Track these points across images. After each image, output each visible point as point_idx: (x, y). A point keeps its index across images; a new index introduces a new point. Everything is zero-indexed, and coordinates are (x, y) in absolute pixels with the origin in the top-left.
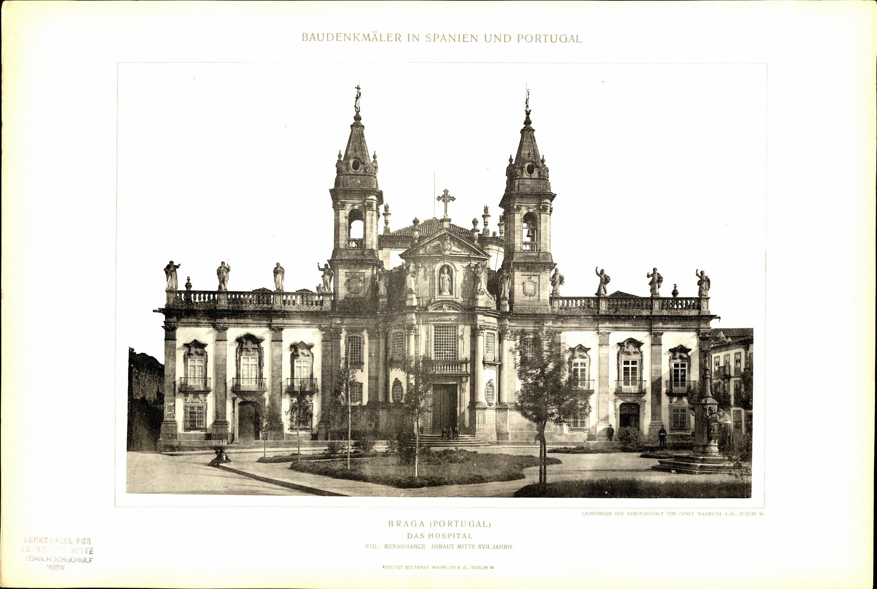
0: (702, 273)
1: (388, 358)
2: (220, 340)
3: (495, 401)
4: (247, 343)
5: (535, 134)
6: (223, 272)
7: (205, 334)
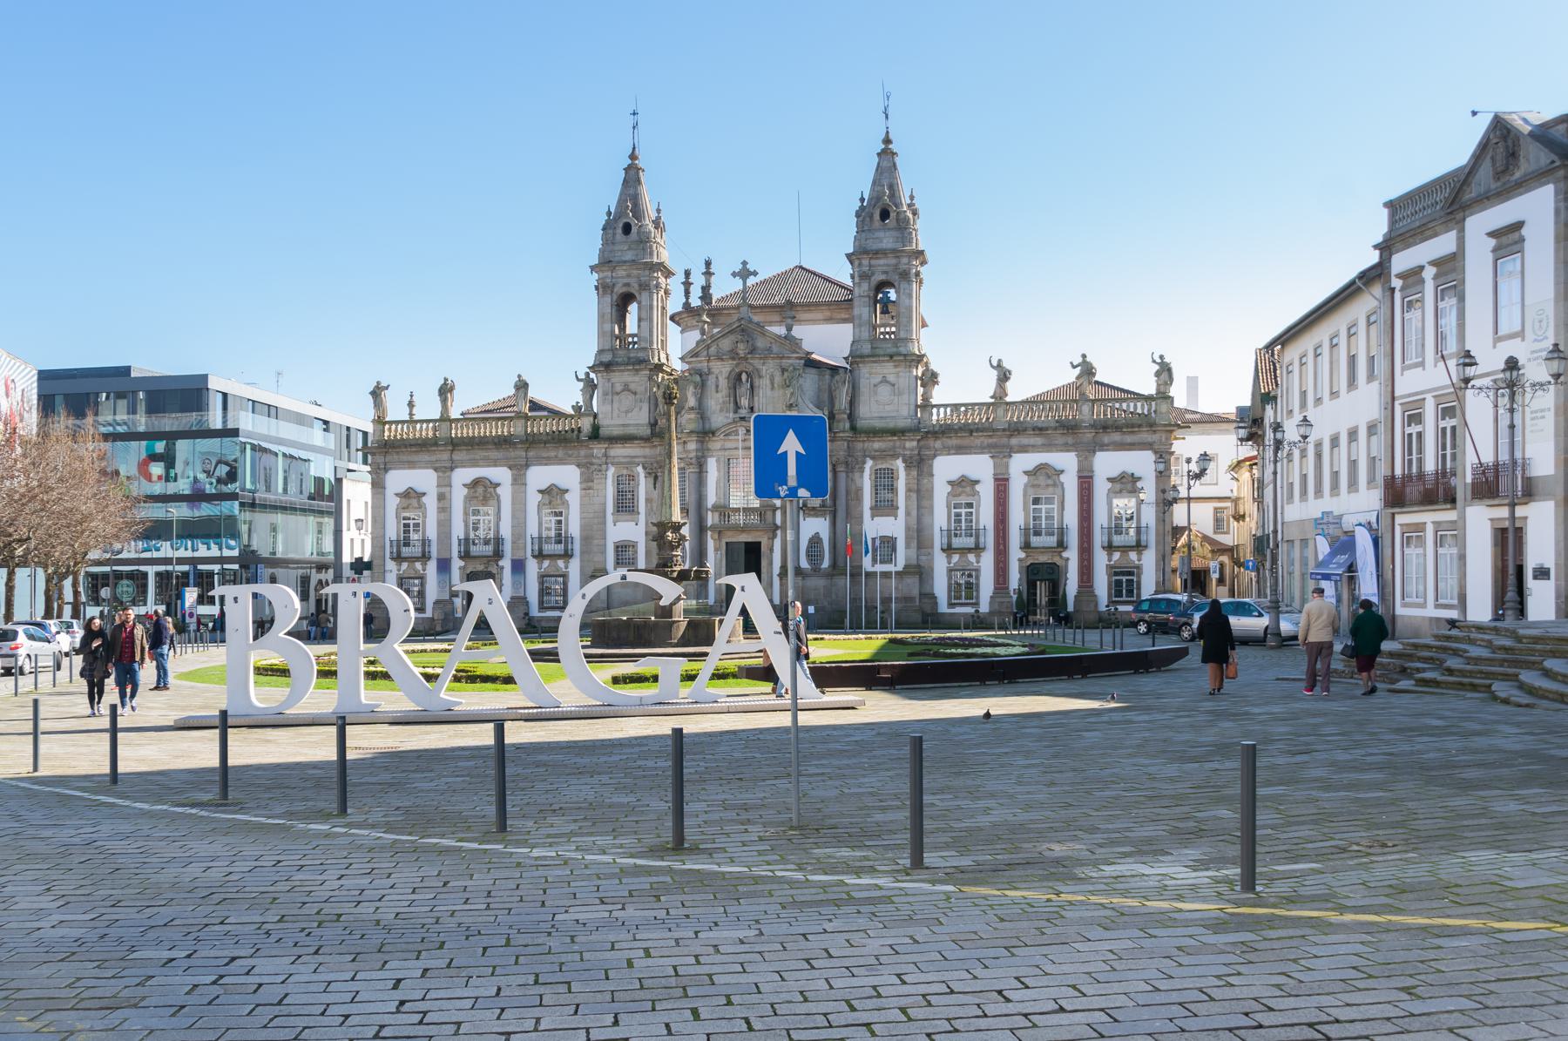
0: (1161, 357)
2: (445, 483)
3: (826, 564)
4: (482, 491)
5: (898, 160)
6: (445, 391)
7: (423, 479)
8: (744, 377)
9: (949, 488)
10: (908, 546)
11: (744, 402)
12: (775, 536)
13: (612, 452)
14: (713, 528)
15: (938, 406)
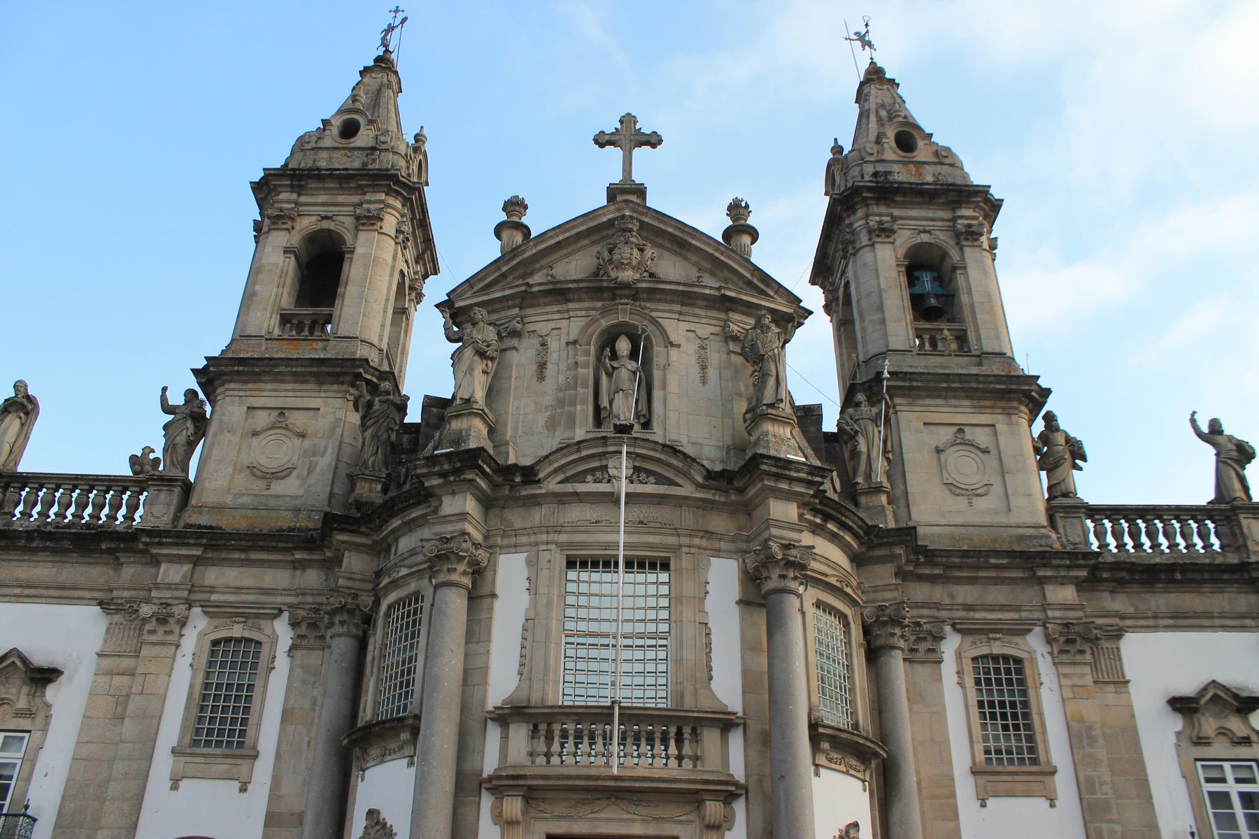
1: (360, 724)
8: (623, 346)
9: (1177, 723)
11: (625, 409)
12: (728, 822)
13: (211, 575)
14: (501, 785)
15: (1096, 512)
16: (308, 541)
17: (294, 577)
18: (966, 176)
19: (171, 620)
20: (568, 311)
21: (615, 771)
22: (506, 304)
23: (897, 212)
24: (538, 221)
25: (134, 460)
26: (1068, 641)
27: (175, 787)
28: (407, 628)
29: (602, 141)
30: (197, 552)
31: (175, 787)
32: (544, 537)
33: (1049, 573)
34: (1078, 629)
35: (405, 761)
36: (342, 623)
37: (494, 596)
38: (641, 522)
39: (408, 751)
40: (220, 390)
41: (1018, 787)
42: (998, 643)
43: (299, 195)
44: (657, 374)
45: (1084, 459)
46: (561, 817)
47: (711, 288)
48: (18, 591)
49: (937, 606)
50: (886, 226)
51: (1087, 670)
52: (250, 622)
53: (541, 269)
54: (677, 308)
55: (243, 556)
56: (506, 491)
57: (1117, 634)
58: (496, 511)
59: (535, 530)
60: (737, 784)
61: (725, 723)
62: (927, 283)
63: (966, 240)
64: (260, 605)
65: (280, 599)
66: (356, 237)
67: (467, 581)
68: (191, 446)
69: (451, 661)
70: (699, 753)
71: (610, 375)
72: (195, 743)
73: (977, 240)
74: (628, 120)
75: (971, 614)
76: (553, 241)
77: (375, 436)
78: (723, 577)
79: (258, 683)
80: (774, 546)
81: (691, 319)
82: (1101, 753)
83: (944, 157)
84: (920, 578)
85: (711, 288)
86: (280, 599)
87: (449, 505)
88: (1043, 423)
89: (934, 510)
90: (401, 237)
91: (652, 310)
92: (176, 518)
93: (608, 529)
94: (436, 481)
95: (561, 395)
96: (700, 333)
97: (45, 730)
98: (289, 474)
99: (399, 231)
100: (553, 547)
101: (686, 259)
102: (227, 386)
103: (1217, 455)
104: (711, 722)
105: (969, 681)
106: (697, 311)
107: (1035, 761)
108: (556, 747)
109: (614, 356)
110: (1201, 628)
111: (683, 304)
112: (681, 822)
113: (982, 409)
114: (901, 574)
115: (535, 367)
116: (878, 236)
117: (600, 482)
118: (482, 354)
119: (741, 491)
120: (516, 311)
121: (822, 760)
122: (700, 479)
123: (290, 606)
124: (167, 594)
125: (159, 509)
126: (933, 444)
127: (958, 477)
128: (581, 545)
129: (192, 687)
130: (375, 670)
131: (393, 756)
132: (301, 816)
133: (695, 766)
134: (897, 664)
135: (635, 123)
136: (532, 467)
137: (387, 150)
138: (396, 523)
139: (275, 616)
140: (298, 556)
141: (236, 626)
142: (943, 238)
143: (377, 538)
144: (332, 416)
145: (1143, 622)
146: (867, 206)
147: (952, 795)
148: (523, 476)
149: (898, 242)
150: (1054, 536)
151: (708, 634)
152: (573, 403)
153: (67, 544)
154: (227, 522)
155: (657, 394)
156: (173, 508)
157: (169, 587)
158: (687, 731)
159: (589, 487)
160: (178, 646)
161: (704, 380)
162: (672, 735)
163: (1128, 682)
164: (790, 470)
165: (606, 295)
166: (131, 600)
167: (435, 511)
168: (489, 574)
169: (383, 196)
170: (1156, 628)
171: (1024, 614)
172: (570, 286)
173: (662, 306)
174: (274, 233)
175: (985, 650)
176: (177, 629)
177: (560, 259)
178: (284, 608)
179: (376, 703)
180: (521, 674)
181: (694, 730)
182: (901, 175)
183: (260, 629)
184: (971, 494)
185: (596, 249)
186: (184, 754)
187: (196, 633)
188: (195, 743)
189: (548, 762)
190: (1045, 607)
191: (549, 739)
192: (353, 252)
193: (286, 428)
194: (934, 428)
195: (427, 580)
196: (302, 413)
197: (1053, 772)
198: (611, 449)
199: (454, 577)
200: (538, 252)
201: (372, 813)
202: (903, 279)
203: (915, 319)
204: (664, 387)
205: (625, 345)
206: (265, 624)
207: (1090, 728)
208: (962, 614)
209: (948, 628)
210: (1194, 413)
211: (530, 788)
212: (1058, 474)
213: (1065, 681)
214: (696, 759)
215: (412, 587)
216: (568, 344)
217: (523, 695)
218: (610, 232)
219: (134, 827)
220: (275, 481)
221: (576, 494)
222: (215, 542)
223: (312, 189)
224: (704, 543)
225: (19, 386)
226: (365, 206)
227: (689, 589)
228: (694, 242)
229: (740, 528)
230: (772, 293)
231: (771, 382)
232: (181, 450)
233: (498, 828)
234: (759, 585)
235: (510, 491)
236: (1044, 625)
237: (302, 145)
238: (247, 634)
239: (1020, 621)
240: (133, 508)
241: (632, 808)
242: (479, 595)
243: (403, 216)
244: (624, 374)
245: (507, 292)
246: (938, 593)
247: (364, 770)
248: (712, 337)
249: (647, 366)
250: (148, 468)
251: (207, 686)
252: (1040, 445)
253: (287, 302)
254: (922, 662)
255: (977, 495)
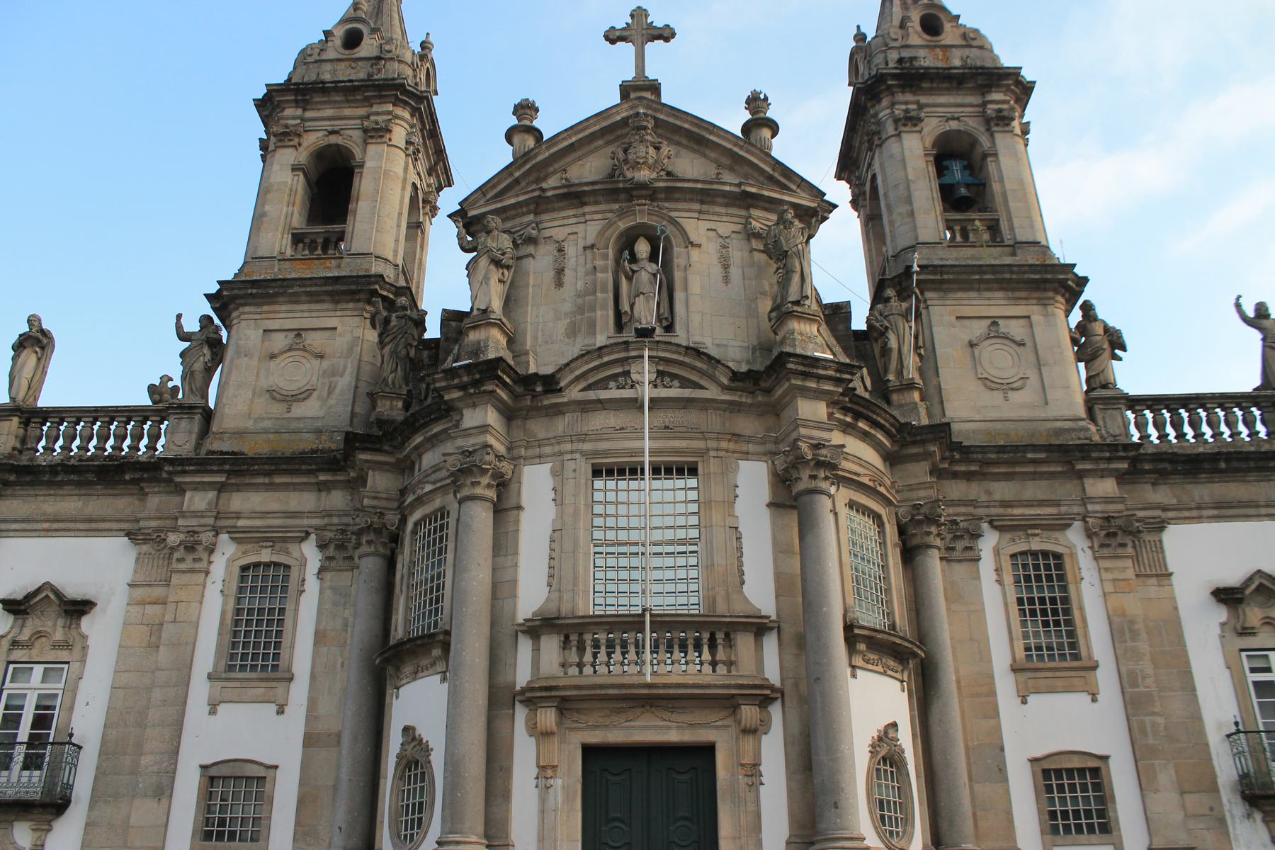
1: (392, 642)
8: (643, 248)
9: (1222, 614)
10: (1145, 783)
11: (646, 312)
13: (236, 501)
14: (534, 697)
15: (1136, 403)
16: (332, 462)
17: (319, 499)
18: (995, 58)
19: (200, 548)
20: (584, 214)
21: (649, 679)
22: (520, 211)
23: (923, 100)
24: (549, 125)
25: (152, 389)
26: (1108, 535)
27: (213, 712)
28: (434, 544)
29: (613, 37)
30: (221, 478)
31: (213, 712)
32: (568, 447)
33: (1088, 466)
34: (1119, 522)
35: (438, 677)
36: (369, 542)
37: (519, 508)
38: (666, 427)
39: (440, 666)
40: (235, 314)
41: (1059, 683)
42: (1037, 539)
43: (304, 110)
44: (678, 275)
45: (1124, 349)
46: (596, 727)
47: (731, 184)
48: (46, 525)
49: (973, 503)
50: (913, 114)
51: (1129, 563)
52: (278, 545)
53: (555, 172)
54: (697, 206)
55: (267, 480)
56: (528, 401)
57: (1160, 526)
58: (519, 422)
59: (559, 440)
60: (772, 688)
61: (759, 628)
62: (956, 172)
63: (997, 125)
64: (286, 529)
65: (306, 522)
66: (365, 151)
67: (491, 494)
68: (209, 372)
69: (478, 575)
70: (733, 658)
71: (630, 279)
72: (231, 668)
73: (1008, 125)
74: (639, 14)
75: (1009, 511)
76: (566, 143)
77: (394, 353)
78: (753, 479)
79: (289, 607)
80: (804, 447)
81: (711, 217)
82: (1143, 646)
83: (972, 39)
84: (955, 475)
85: (731, 184)
86: (306, 522)
87: (471, 418)
88: (1080, 313)
89: (969, 405)
90: (411, 148)
91: (671, 210)
92: (198, 445)
93: (634, 435)
94: (456, 394)
95: (580, 301)
96: (721, 231)
97: (83, 660)
98: (309, 396)
99: (408, 143)
100: (577, 456)
101: (704, 156)
102: (241, 310)
103: (1264, 340)
104: (744, 627)
105: (1008, 579)
106: (718, 209)
107: (1076, 657)
108: (588, 657)
109: (634, 259)
110: (1247, 517)
111: (702, 202)
112: (717, 727)
113: (1016, 301)
114: (936, 472)
115: (552, 274)
116: (905, 125)
117: (623, 387)
118: (497, 263)
119: (768, 391)
120: (531, 217)
121: (858, 661)
122: (725, 381)
123: (317, 528)
124: (194, 522)
125: (180, 438)
126: (966, 338)
127: (993, 372)
128: (606, 453)
129: (223, 613)
130: (404, 588)
131: (426, 673)
132: (339, 735)
133: (729, 671)
134: (933, 564)
135: (647, 16)
136: (553, 376)
137: (392, 59)
138: (418, 439)
139: (303, 539)
140: (322, 477)
141: (264, 551)
142: (973, 125)
143: (401, 456)
144: (350, 335)
145: (1186, 514)
146: (892, 94)
147: (993, 693)
148: (544, 385)
149: (926, 130)
150: (1093, 428)
151: (739, 539)
152: (593, 309)
153: (91, 477)
154: (249, 447)
155: (679, 296)
156: (194, 436)
157: (195, 514)
158: (720, 636)
159: (613, 393)
160: (207, 573)
161: (726, 279)
162: (705, 641)
163: (1171, 574)
164: (818, 368)
165: (622, 196)
166: (158, 530)
167: (457, 426)
168: (514, 486)
169: (390, 107)
170: (1199, 519)
171: (1063, 509)
172: (586, 188)
173: (680, 206)
174: (281, 152)
175: (1023, 547)
176: (205, 556)
177: (574, 161)
178: (310, 530)
179: (407, 622)
180: (550, 585)
181: (727, 635)
182: (927, 60)
183: (287, 553)
184: (1007, 388)
185: (610, 149)
186: (219, 679)
187: (225, 558)
188: (231, 668)
189: (581, 672)
190: (1084, 501)
191: (581, 649)
192: (362, 166)
193: (304, 349)
194: (967, 322)
195: (452, 495)
196: (319, 333)
197: (1095, 667)
198: (633, 353)
199: (478, 491)
200: (552, 155)
201: (407, 730)
202: (932, 169)
203: (945, 210)
204: (686, 289)
205: (645, 247)
206: (292, 547)
207: (1132, 622)
208: (1000, 511)
209: (985, 526)
210: (1239, 297)
211: (564, 699)
212: (1097, 365)
213: (1105, 575)
214: (730, 664)
215: (437, 503)
216: (585, 248)
217: (553, 606)
218: (625, 131)
219: (176, 752)
220: (295, 404)
221: (599, 401)
222: (239, 468)
223: (320, 103)
224: (732, 446)
225: (33, 320)
226: (372, 118)
227: (718, 493)
228: (712, 138)
229: (768, 430)
230: (794, 187)
231: (796, 278)
232: (199, 377)
233: (533, 739)
234: (789, 486)
235: (532, 401)
236: (1084, 520)
237: (304, 58)
238: (275, 558)
239: (1060, 516)
240: (154, 437)
241: (667, 715)
242: (505, 508)
243: (412, 126)
244: (644, 276)
245: (521, 198)
246: (974, 490)
247: (398, 688)
248: (734, 235)
249: (667, 268)
250: (167, 396)
251: (238, 611)
252: (1077, 336)
253: (298, 221)
254: (960, 561)
255: (1013, 389)
